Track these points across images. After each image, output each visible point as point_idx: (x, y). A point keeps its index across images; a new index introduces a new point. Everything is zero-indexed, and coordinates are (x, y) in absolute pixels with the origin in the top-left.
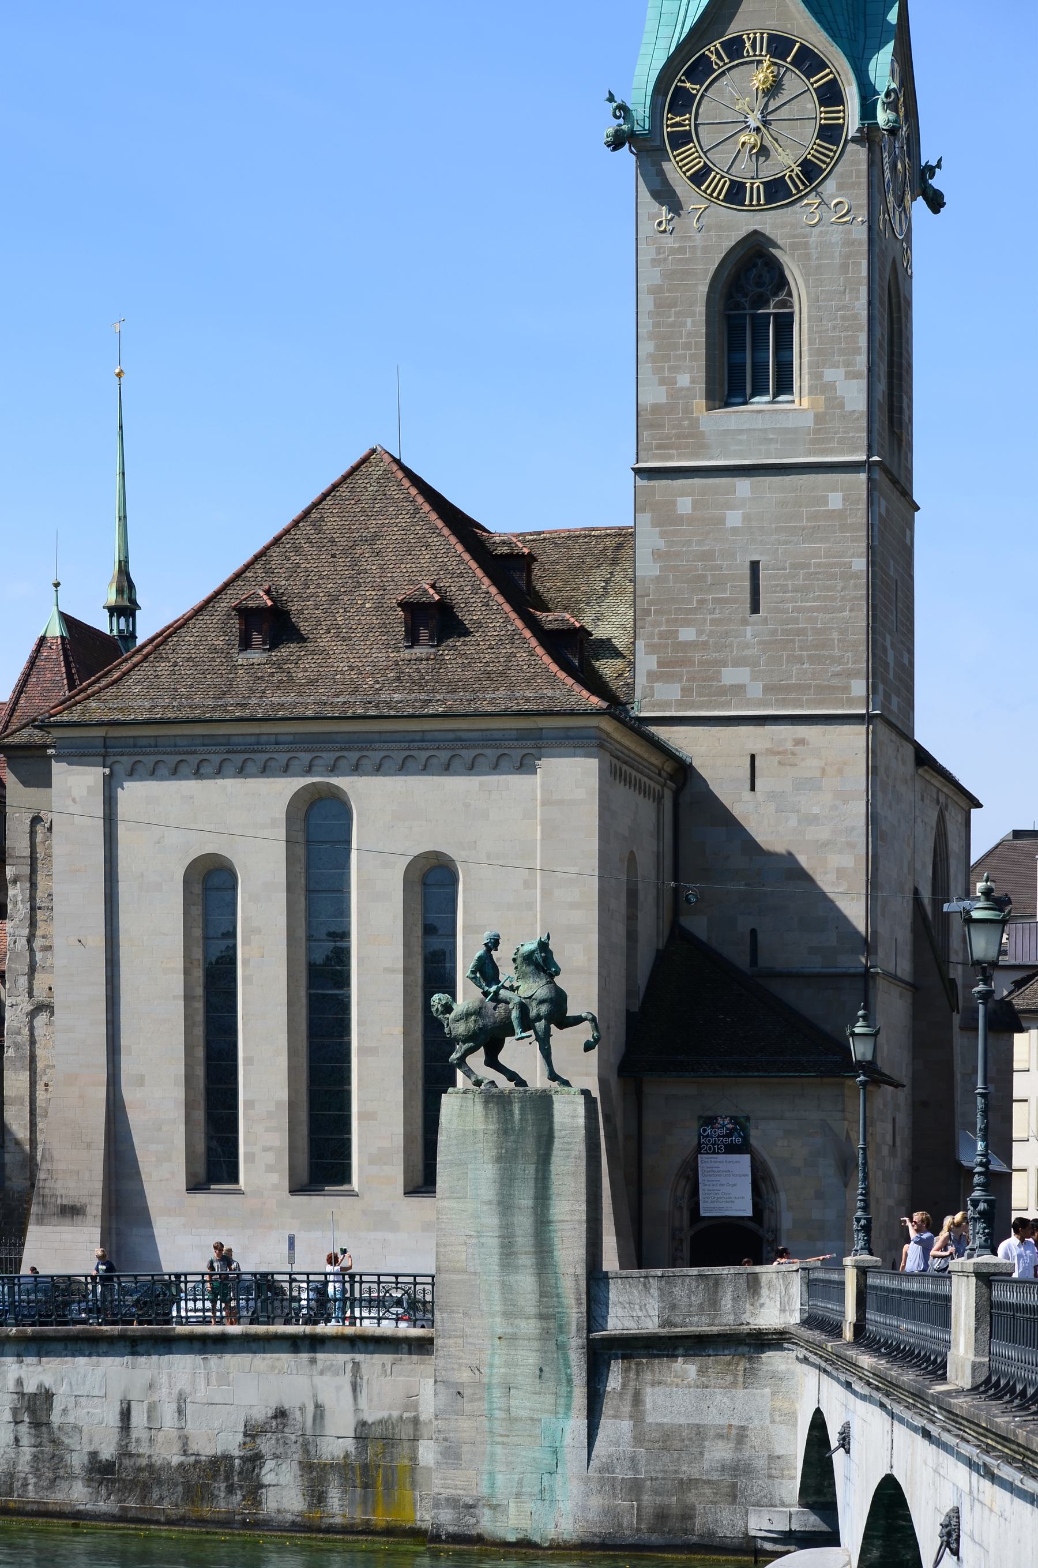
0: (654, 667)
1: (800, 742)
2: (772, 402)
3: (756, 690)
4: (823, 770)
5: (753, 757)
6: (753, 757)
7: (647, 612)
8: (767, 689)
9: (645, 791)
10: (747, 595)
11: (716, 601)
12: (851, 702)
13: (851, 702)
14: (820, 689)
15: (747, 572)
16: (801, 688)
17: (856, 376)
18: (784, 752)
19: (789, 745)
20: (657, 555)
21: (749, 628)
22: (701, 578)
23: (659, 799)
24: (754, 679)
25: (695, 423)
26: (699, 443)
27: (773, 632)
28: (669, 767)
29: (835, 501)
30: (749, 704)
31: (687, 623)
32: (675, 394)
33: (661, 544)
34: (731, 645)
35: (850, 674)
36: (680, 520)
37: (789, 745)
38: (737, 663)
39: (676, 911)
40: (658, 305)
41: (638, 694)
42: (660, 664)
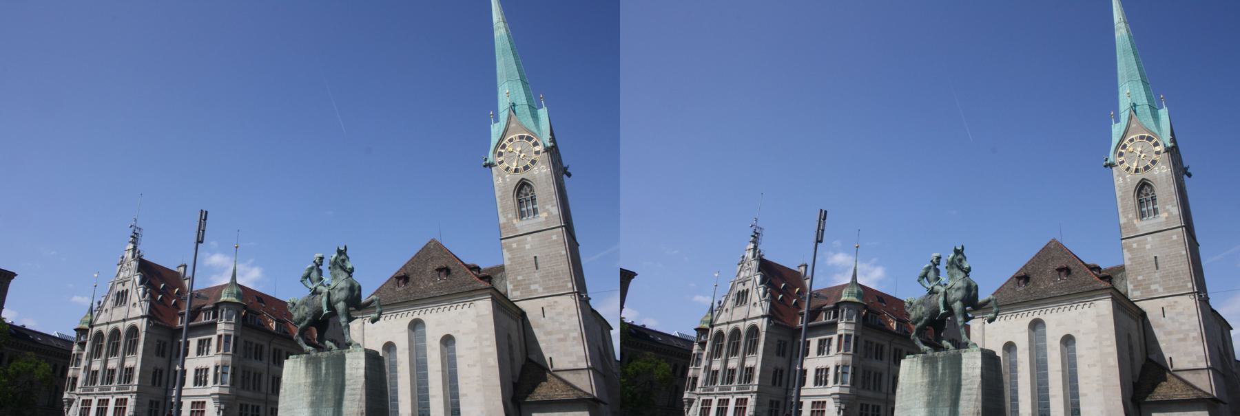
0: (512, 287)
1: (556, 302)
2: (534, 217)
3: (540, 290)
4: (564, 309)
5: (543, 308)
6: (543, 308)
7: (508, 274)
8: (544, 289)
9: (513, 318)
10: (534, 265)
11: (527, 268)
12: (568, 289)
13: (568, 289)
14: (559, 287)
15: (533, 259)
16: (553, 287)
17: (555, 206)
18: (551, 306)
19: (552, 304)
20: (509, 259)
21: (536, 274)
22: (522, 263)
23: (517, 322)
24: (540, 286)
25: (514, 225)
26: (517, 230)
27: (543, 274)
28: (519, 312)
29: (554, 237)
30: (538, 294)
31: (519, 275)
32: (508, 220)
33: (510, 256)
34: (532, 279)
35: (567, 281)
36: (513, 250)
37: (552, 304)
38: (535, 283)
39: (527, 354)
40: (501, 200)
41: (509, 295)
42: (514, 286)
